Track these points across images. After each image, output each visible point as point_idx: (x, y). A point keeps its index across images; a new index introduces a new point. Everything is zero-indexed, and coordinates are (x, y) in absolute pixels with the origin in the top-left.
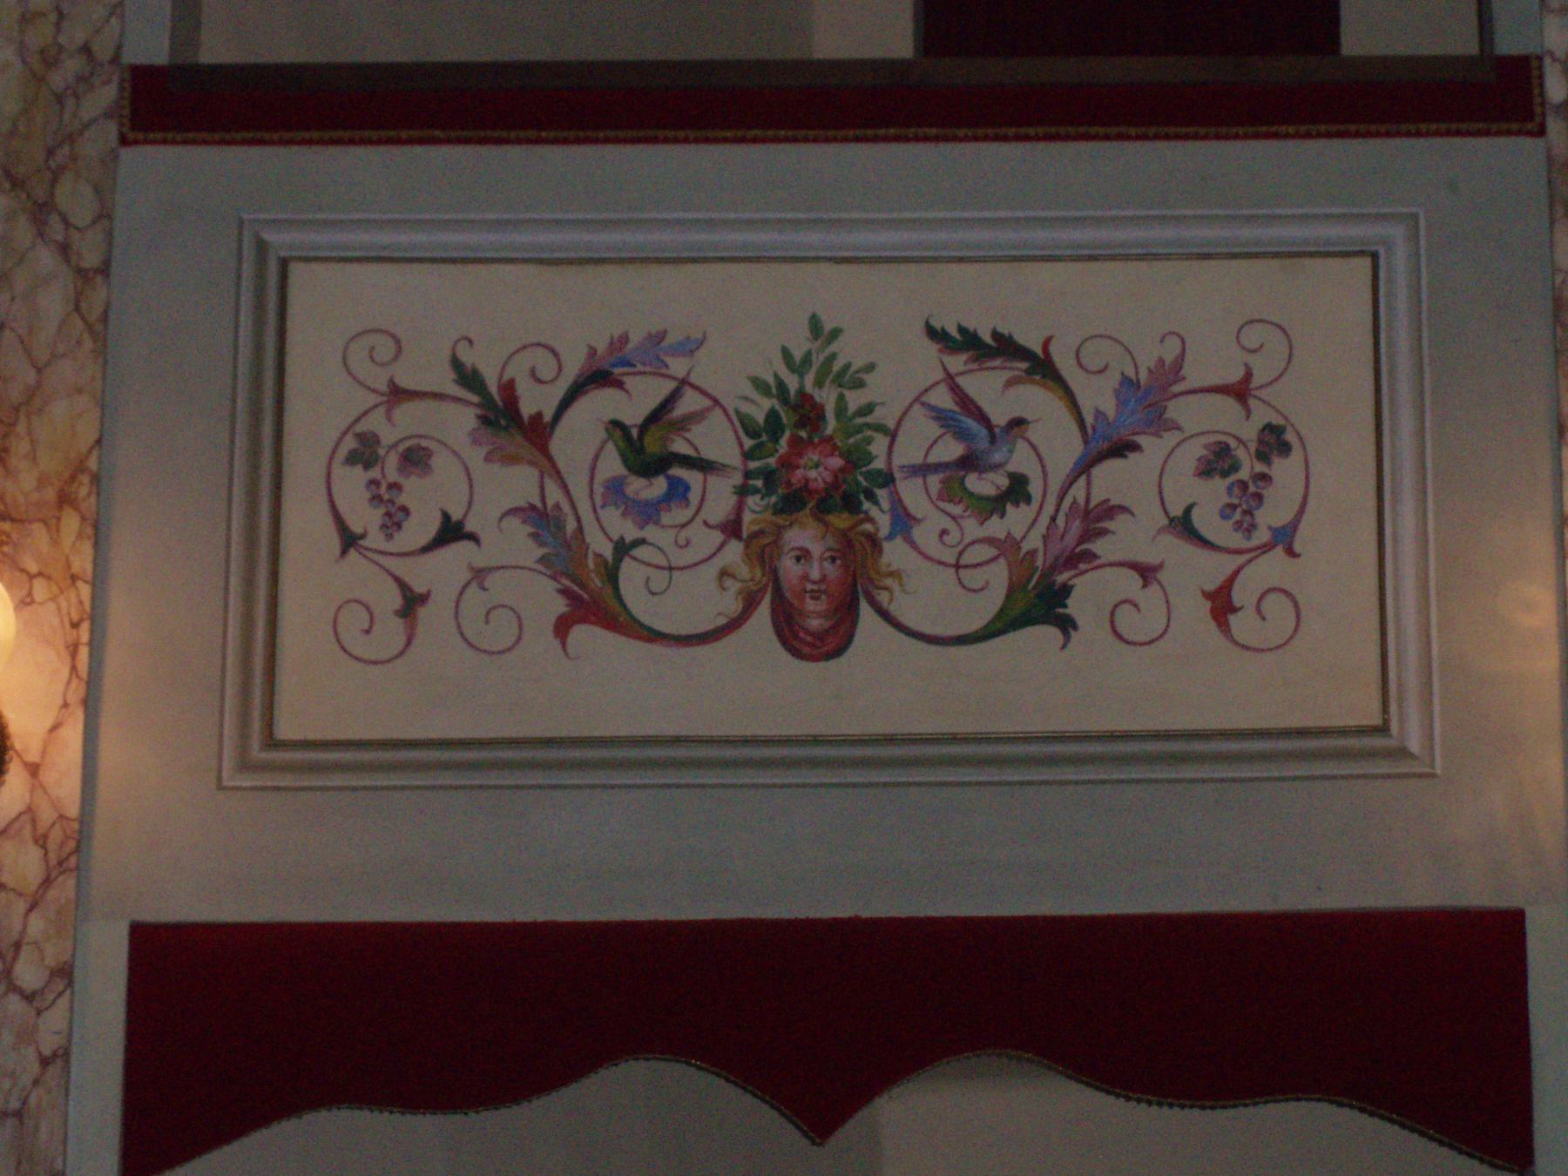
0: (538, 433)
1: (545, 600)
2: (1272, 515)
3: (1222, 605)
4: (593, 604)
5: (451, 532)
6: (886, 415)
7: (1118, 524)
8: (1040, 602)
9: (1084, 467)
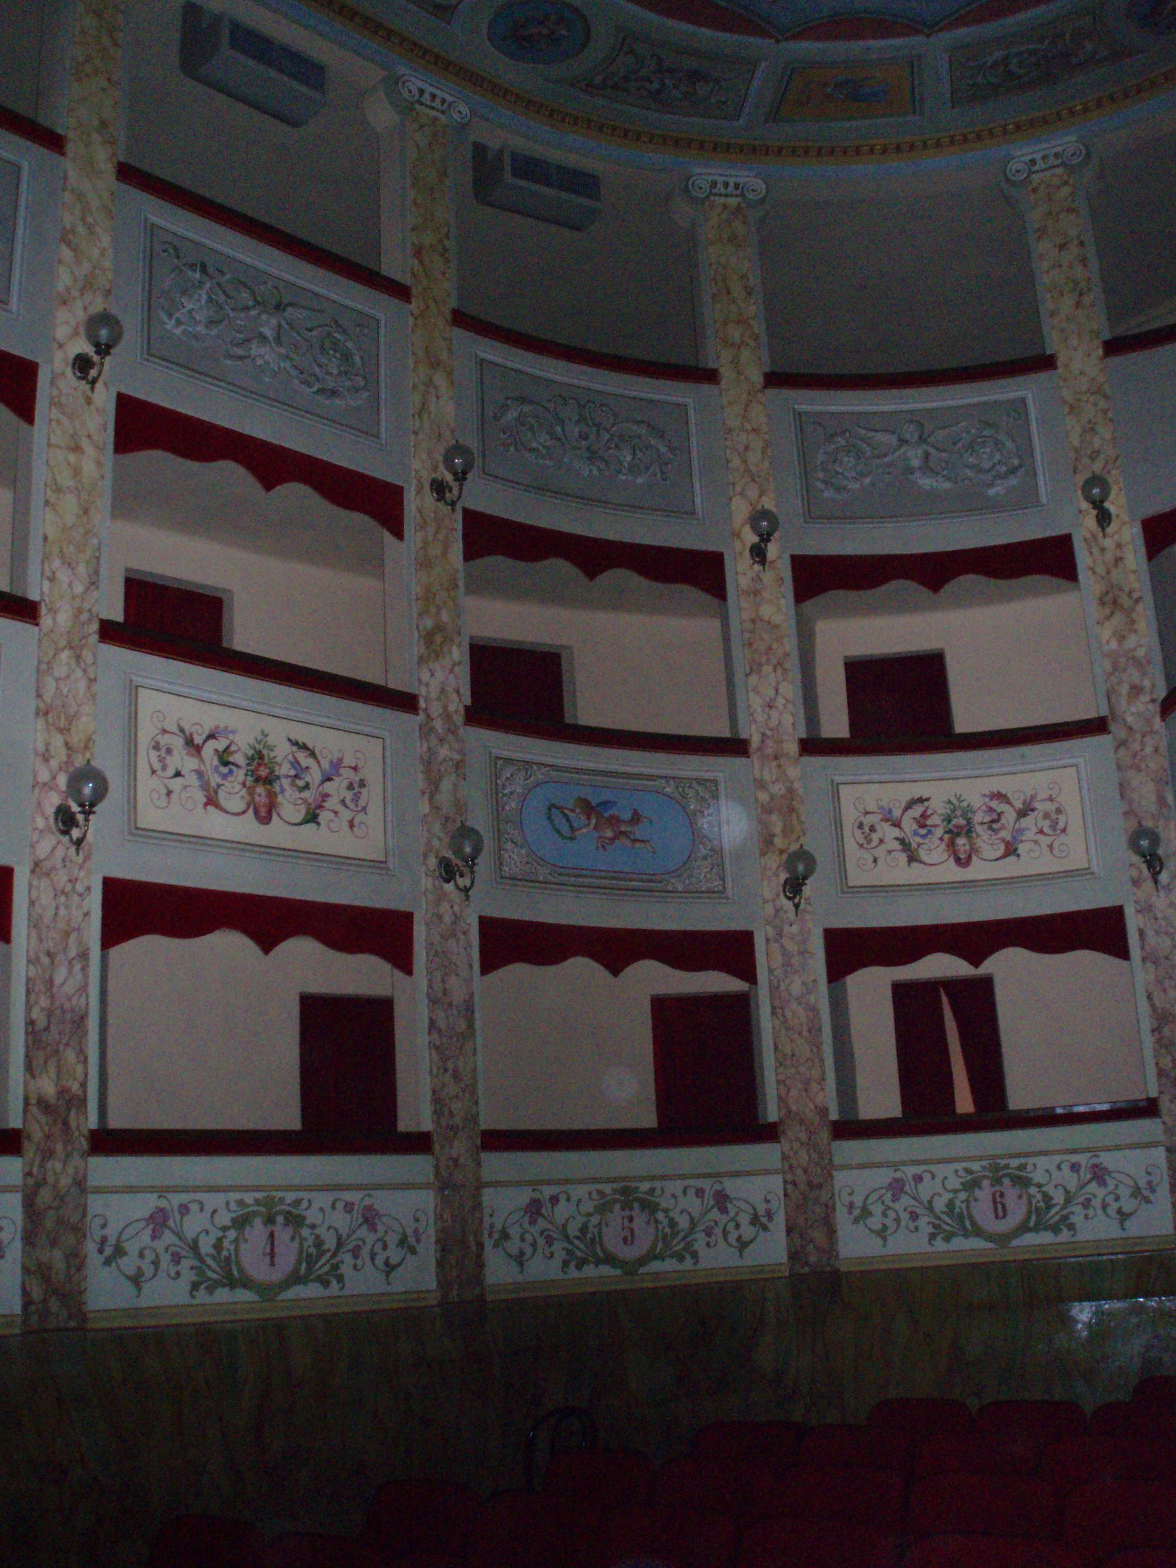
0: (198, 749)
1: (201, 797)
2: (362, 803)
3: (351, 825)
4: (212, 801)
5: (178, 774)
6: (279, 760)
7: (329, 799)
8: (312, 818)
9: (323, 782)
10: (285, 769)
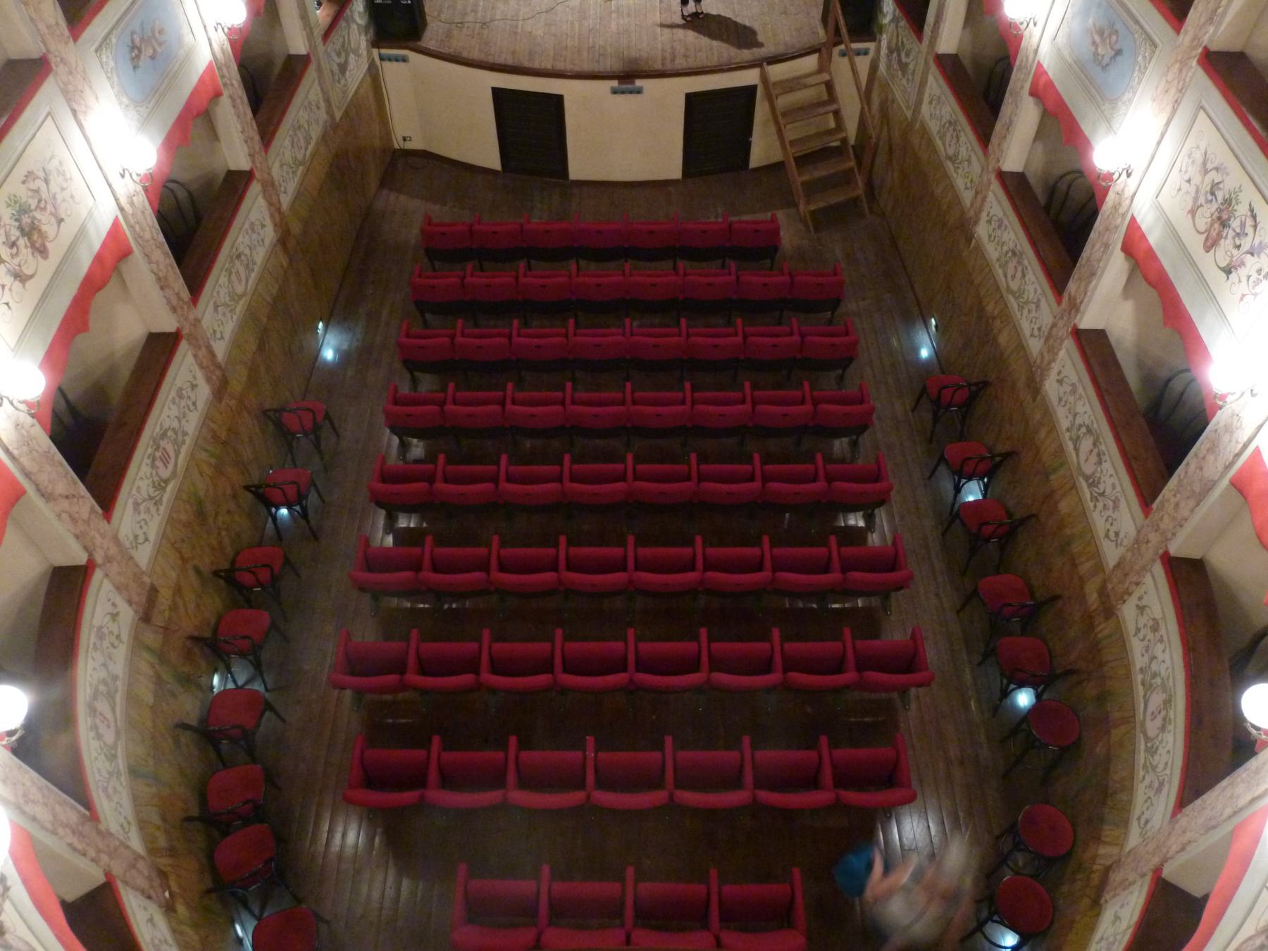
0: (1206, 172)
2: (1258, 289)
9: (1248, 252)
10: (1235, 224)
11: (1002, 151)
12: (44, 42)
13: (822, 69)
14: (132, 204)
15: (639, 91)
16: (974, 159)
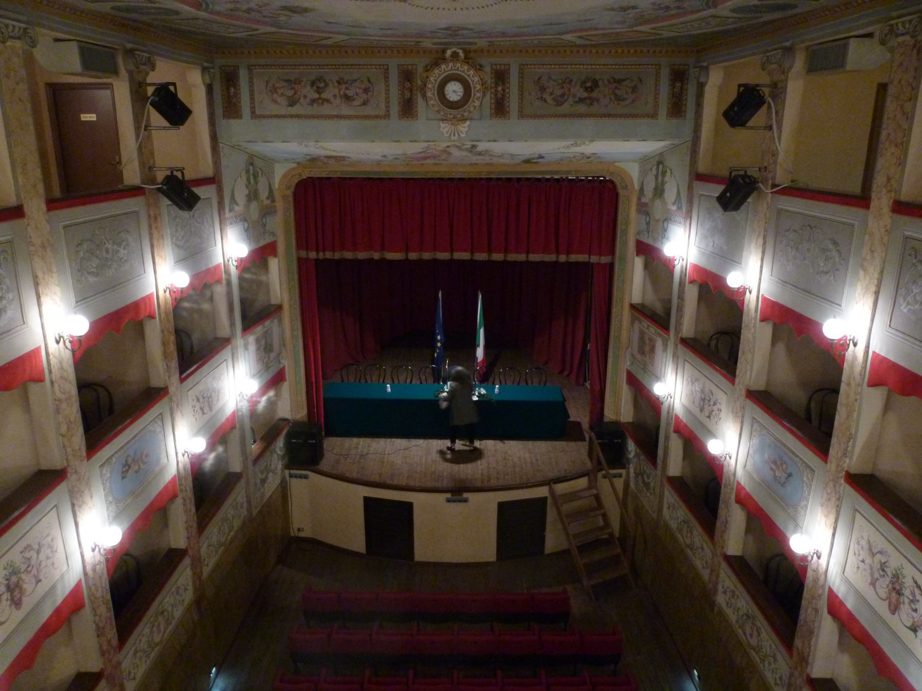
10: (907, 592)
11: (724, 541)
12: (67, 460)
13: (590, 487)
14: (94, 570)
15: (466, 501)
16: (705, 546)
